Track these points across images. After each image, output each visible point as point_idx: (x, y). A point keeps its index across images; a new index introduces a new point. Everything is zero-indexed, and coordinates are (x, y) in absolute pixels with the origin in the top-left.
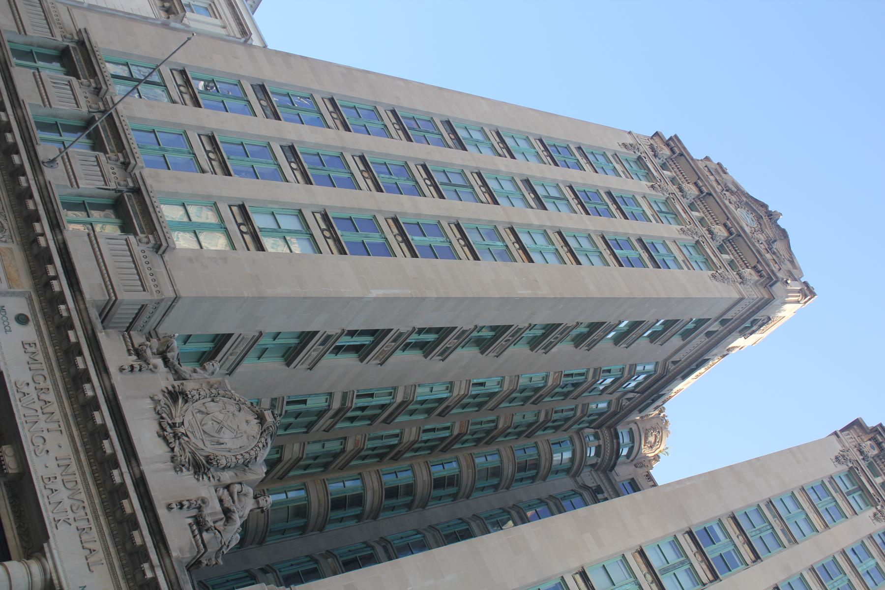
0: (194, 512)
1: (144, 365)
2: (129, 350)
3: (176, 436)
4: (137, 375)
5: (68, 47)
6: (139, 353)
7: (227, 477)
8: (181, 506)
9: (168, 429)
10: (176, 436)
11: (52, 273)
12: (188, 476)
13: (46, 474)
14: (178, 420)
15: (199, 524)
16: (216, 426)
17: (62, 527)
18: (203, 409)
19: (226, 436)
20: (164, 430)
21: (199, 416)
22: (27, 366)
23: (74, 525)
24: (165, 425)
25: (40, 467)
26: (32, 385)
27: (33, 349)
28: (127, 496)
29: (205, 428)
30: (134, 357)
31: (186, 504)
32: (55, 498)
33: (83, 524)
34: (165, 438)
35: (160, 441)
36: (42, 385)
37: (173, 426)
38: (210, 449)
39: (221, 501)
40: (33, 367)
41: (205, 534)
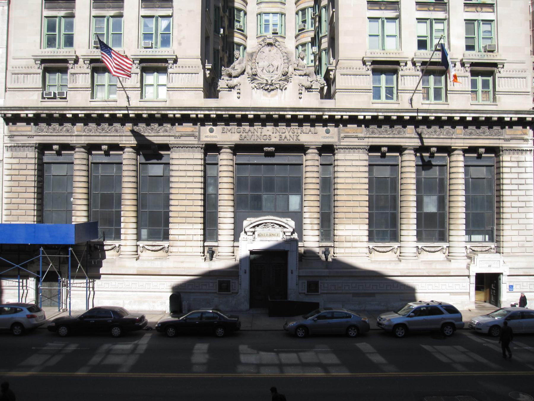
0: (304, 88)
1: (238, 87)
2: (229, 91)
3: (271, 85)
4: (241, 91)
5: (44, 68)
6: (231, 88)
7: (291, 70)
8: (301, 93)
9: (268, 86)
10: (271, 85)
11: (195, 116)
12: (289, 86)
13: (278, 138)
14: (265, 82)
15: (309, 89)
16: (271, 66)
17: (299, 138)
18: (261, 69)
19: (276, 64)
20: (268, 89)
21: (264, 71)
22: (233, 134)
23: (299, 134)
24: (266, 88)
25: (275, 140)
26: (241, 134)
27: (225, 130)
28: (297, 115)
29: (271, 71)
30: (232, 90)
31: (300, 91)
32: (288, 137)
33: (299, 131)
34: (273, 90)
35: (272, 92)
36: (242, 130)
37: (267, 84)
38: (280, 72)
39: (300, 75)
40: (233, 131)
41: (313, 87)
